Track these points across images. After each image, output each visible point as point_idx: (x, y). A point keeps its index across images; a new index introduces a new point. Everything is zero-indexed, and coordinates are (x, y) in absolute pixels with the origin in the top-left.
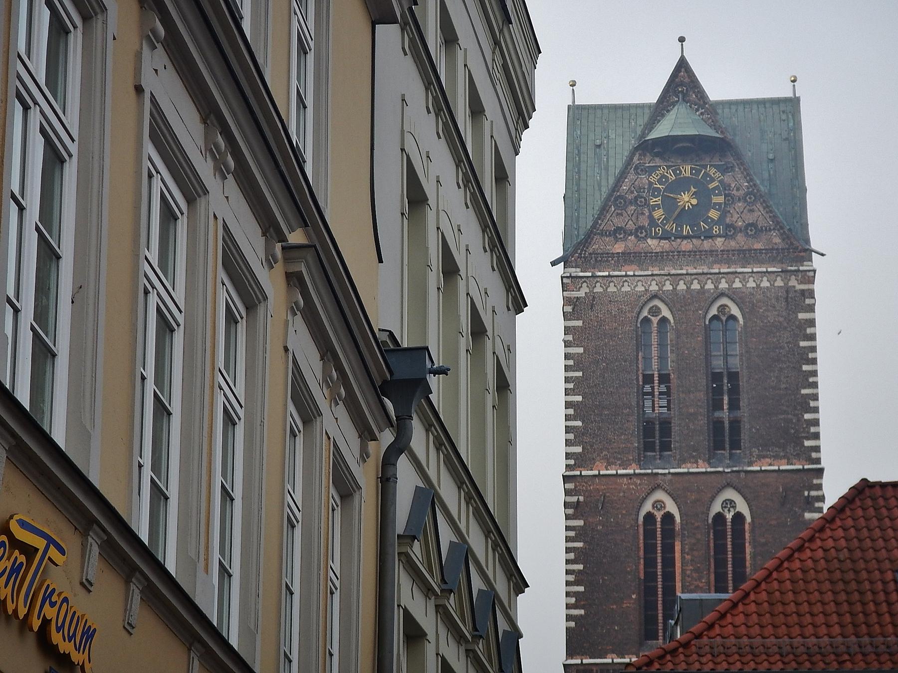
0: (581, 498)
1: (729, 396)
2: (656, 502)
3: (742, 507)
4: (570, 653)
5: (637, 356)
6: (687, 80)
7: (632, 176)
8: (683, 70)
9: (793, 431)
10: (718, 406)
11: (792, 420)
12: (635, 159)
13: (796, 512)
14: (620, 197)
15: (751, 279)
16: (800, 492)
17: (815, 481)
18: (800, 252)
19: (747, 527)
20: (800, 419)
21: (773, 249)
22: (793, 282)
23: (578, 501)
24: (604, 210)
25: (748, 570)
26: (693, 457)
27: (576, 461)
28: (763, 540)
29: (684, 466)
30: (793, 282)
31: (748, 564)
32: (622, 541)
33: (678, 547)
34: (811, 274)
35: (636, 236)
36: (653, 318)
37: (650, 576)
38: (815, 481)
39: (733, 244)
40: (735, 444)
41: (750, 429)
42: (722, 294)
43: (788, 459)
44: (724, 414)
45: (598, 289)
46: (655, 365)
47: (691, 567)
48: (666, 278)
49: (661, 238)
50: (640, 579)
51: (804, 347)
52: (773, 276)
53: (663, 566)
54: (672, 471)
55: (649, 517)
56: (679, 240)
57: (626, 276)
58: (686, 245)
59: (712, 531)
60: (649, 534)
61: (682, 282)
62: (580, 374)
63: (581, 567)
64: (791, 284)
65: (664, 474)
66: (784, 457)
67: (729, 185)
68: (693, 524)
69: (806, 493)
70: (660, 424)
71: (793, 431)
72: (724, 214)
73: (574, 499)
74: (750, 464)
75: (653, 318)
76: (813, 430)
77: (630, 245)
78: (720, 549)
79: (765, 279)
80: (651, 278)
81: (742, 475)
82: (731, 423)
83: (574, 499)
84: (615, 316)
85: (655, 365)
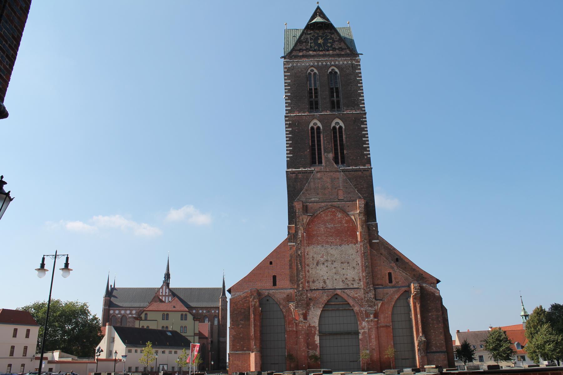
0: (291, 122)
1: (336, 93)
2: (314, 123)
3: (342, 124)
4: (288, 168)
5: (307, 83)
6: (320, 12)
7: (304, 35)
9: (356, 102)
10: (333, 96)
11: (355, 99)
12: (305, 31)
15: (341, 62)
17: (364, 116)
18: (355, 55)
19: (343, 130)
20: (358, 99)
21: (347, 54)
23: (290, 123)
24: (296, 45)
25: (344, 143)
27: (289, 111)
28: (349, 133)
30: (354, 62)
31: (344, 140)
33: (322, 136)
34: (359, 60)
35: (306, 51)
37: (313, 145)
38: (364, 116)
39: (335, 53)
40: (339, 107)
41: (343, 102)
43: (355, 110)
44: (335, 99)
45: (295, 65)
46: (313, 85)
47: (326, 141)
49: (314, 51)
50: (310, 146)
51: (358, 80)
52: (348, 61)
53: (317, 142)
55: (312, 128)
56: (319, 52)
57: (303, 61)
58: (321, 53)
59: (332, 131)
60: (313, 133)
61: (320, 63)
62: (290, 87)
63: (291, 142)
64: (353, 63)
65: (316, 115)
66: (354, 110)
67: (333, 38)
68: (326, 129)
69: (361, 120)
70: (315, 101)
71: (356, 102)
72: (332, 45)
73: (288, 122)
74: (344, 112)
75: (312, 73)
76: (362, 102)
77: (304, 53)
78: (335, 137)
79: (345, 62)
80: (311, 61)
81: (341, 114)
82: (337, 101)
83: (288, 122)
84: (300, 72)
85: (313, 85)
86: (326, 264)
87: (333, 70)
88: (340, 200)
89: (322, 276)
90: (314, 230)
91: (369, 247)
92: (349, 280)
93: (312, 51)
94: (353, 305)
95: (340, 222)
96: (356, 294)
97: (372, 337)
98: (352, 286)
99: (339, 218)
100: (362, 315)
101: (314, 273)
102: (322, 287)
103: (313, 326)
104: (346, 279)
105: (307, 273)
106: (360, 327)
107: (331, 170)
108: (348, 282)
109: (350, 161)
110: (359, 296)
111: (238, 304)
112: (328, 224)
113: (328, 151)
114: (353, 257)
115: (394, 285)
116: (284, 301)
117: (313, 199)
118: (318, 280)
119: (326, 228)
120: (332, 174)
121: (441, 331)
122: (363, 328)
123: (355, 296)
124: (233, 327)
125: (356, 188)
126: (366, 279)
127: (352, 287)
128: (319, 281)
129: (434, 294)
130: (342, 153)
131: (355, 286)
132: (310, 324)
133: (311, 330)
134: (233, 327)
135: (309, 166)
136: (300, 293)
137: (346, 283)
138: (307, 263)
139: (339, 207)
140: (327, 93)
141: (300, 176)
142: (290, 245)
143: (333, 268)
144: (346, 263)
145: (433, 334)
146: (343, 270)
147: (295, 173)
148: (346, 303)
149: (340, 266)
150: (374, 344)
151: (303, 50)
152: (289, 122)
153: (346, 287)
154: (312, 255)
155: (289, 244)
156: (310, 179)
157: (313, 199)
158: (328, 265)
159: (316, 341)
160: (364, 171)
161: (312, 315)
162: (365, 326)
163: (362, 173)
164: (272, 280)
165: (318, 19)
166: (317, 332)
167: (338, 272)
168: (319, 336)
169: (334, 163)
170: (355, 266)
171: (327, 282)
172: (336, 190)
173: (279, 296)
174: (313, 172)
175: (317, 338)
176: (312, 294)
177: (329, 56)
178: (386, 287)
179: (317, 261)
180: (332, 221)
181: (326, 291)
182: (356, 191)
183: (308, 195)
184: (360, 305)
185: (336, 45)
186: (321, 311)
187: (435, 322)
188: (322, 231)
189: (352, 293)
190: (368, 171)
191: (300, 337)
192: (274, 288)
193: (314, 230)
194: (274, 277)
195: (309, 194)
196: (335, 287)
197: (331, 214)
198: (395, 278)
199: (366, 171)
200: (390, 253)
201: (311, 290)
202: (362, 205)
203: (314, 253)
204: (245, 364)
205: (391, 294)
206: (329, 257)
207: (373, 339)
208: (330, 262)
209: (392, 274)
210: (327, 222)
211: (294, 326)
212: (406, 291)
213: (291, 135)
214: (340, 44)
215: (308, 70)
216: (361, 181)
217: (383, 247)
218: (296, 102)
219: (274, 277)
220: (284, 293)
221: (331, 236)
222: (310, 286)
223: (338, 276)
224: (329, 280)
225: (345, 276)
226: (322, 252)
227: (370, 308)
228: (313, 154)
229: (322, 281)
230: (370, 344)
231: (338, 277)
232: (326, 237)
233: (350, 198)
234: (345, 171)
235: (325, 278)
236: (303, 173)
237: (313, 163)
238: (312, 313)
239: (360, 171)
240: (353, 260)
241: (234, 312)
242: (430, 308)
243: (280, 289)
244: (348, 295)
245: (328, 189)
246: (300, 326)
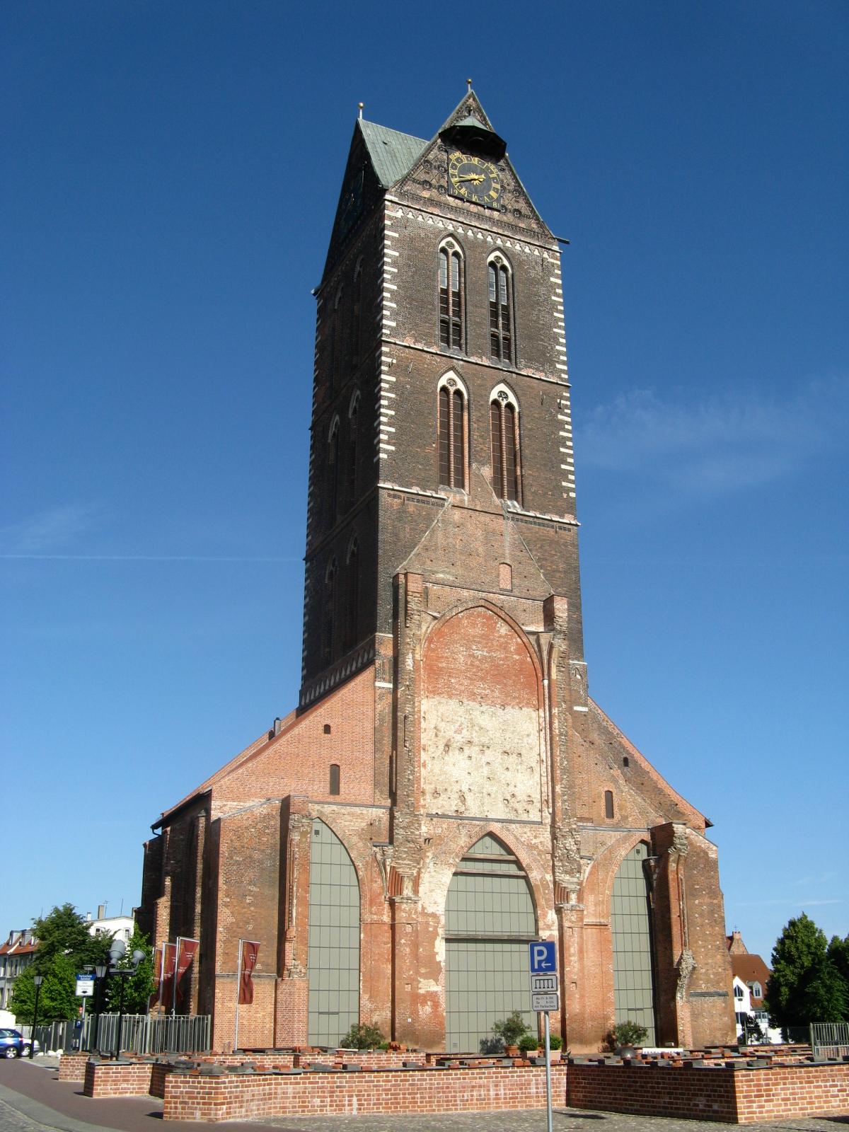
0: (395, 361)
3: (512, 399)
7: (435, 151)
8: (472, 99)
13: (552, 413)
14: (427, 161)
16: (554, 399)
22: (546, 255)
24: (416, 166)
26: (479, 353)
29: (472, 358)
30: (546, 255)
32: (426, 400)
35: (438, 191)
36: (449, 250)
39: (505, 218)
42: (499, 249)
43: (546, 373)
45: (410, 216)
48: (460, 224)
49: (456, 197)
51: (555, 301)
54: (464, 359)
56: (468, 204)
57: (432, 214)
58: (473, 208)
60: (445, 404)
62: (396, 270)
63: (393, 413)
66: (543, 371)
69: (558, 401)
74: (520, 369)
77: (433, 194)
86: (467, 752)
88: (503, 592)
89: (457, 782)
90: (442, 657)
91: (570, 721)
92: (518, 799)
95: (505, 647)
96: (535, 837)
97: (572, 950)
98: (526, 815)
99: (501, 636)
100: (547, 891)
101: (437, 771)
102: (457, 811)
103: (433, 913)
104: (513, 795)
105: (422, 769)
107: (486, 510)
108: (517, 806)
109: (531, 498)
110: (541, 842)
111: (245, 835)
112: (474, 647)
113: (482, 459)
114: (530, 741)
115: (617, 824)
116: (360, 838)
117: (441, 576)
118: (446, 789)
119: (470, 655)
120: (487, 518)
121: (718, 943)
123: (533, 842)
124: (229, 900)
125: (541, 567)
126: (564, 801)
127: (524, 817)
128: (449, 793)
129: (706, 854)
130: (512, 472)
131: (534, 816)
132: (423, 908)
133: (427, 923)
134: (229, 900)
135: (434, 488)
136: (406, 820)
137: (512, 807)
138: (423, 742)
139: (501, 608)
140: (486, 312)
141: (411, 507)
142: (380, 688)
143: (484, 765)
144: (514, 755)
145: (703, 950)
146: (508, 773)
147: (399, 497)
148: (512, 858)
149: (499, 760)
150: (576, 969)
152: (389, 360)
153: (512, 816)
154: (435, 721)
155: (378, 684)
156: (436, 521)
157: (441, 576)
158: (473, 755)
159: (437, 953)
160: (560, 528)
161: (430, 882)
163: (556, 532)
164: (329, 779)
166: (441, 931)
167: (496, 777)
168: (448, 940)
169: (494, 494)
170: (534, 765)
171: (469, 797)
172: (496, 563)
173: (347, 823)
174: (443, 505)
175: (440, 947)
176: (432, 828)
178: (598, 826)
179: (445, 741)
180: (485, 642)
181: (467, 821)
182: (542, 575)
183: (429, 562)
184: (543, 867)
186: (451, 875)
187: (706, 921)
188: (460, 663)
189: (525, 833)
190: (569, 530)
191: (403, 941)
192: (331, 798)
193: (442, 657)
194: (335, 770)
195: (432, 561)
196: (486, 814)
197: (483, 623)
198: (620, 809)
199: (565, 529)
200: (611, 744)
201: (431, 817)
202: (563, 613)
203: (440, 719)
204: (257, 1012)
205: (612, 845)
206: (474, 734)
207: (574, 955)
208: (477, 748)
209: (614, 794)
210: (474, 641)
211: (383, 910)
213: (393, 396)
214: (516, 201)
215: (442, 240)
216: (553, 552)
217: (595, 726)
218: (409, 313)
219: (335, 770)
220: (361, 816)
221: (482, 679)
222: (427, 806)
223: (492, 785)
224: (472, 794)
225: (511, 788)
226: (460, 719)
227: (567, 877)
228: (445, 458)
229: (456, 796)
230: (568, 969)
231: (495, 788)
232: (470, 679)
233: (528, 590)
234: (518, 520)
235: (465, 788)
236: (418, 501)
237: (445, 481)
238: (431, 879)
239: (553, 527)
240: (531, 749)
241: (232, 858)
242: (696, 887)
243: (349, 805)
244: (517, 839)
245: (478, 555)
246: (404, 911)
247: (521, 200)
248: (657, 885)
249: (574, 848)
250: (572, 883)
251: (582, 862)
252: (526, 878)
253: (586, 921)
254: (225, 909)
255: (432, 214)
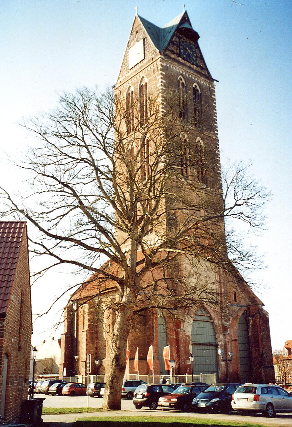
7: (175, 37)
30: (211, 86)
45: (168, 65)
58: (188, 64)
87: (196, 86)
93: (181, 58)
94: (214, 318)
106: (218, 340)
122: (221, 341)
133: (187, 339)
148: (209, 315)
151: (174, 53)
162: (222, 339)
165: (186, 25)
166: (191, 342)
168: (192, 345)
175: (191, 347)
177: (193, 69)
185: (199, 62)
212: (245, 310)
227: (226, 323)
247: (202, 61)
248: (251, 326)
249: (228, 312)
250: (228, 325)
251: (230, 317)
252: (213, 323)
253: (233, 339)
254: (131, 334)
255: (175, 65)
